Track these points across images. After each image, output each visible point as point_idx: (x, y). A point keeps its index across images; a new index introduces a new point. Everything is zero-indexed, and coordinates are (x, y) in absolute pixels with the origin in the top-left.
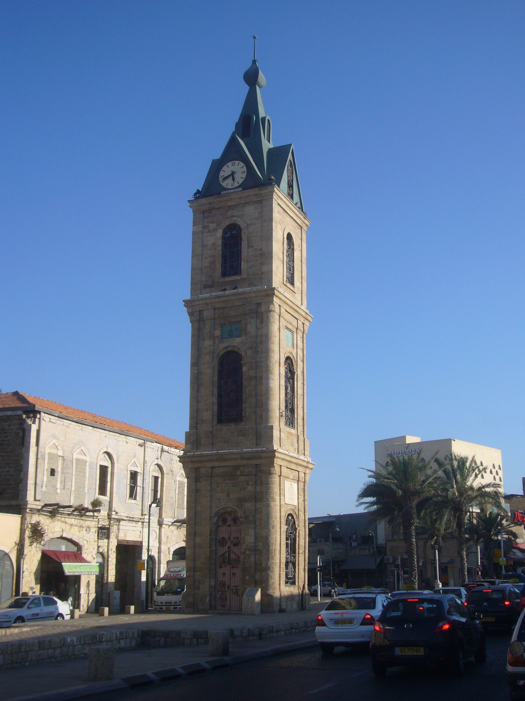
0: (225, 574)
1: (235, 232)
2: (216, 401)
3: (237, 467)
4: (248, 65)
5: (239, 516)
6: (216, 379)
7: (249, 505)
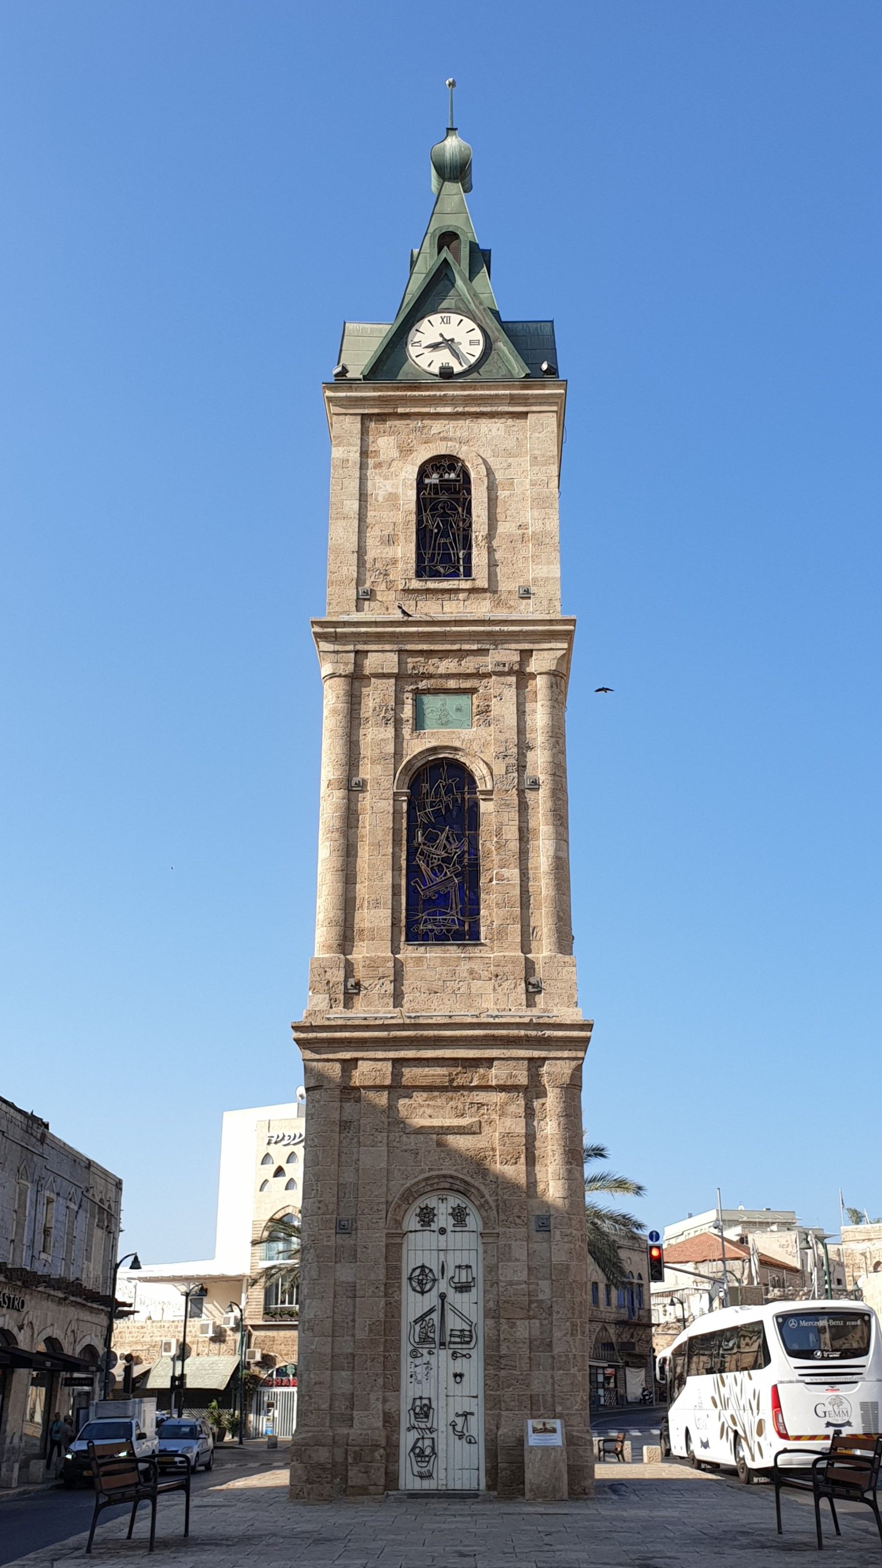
1: (453, 476)
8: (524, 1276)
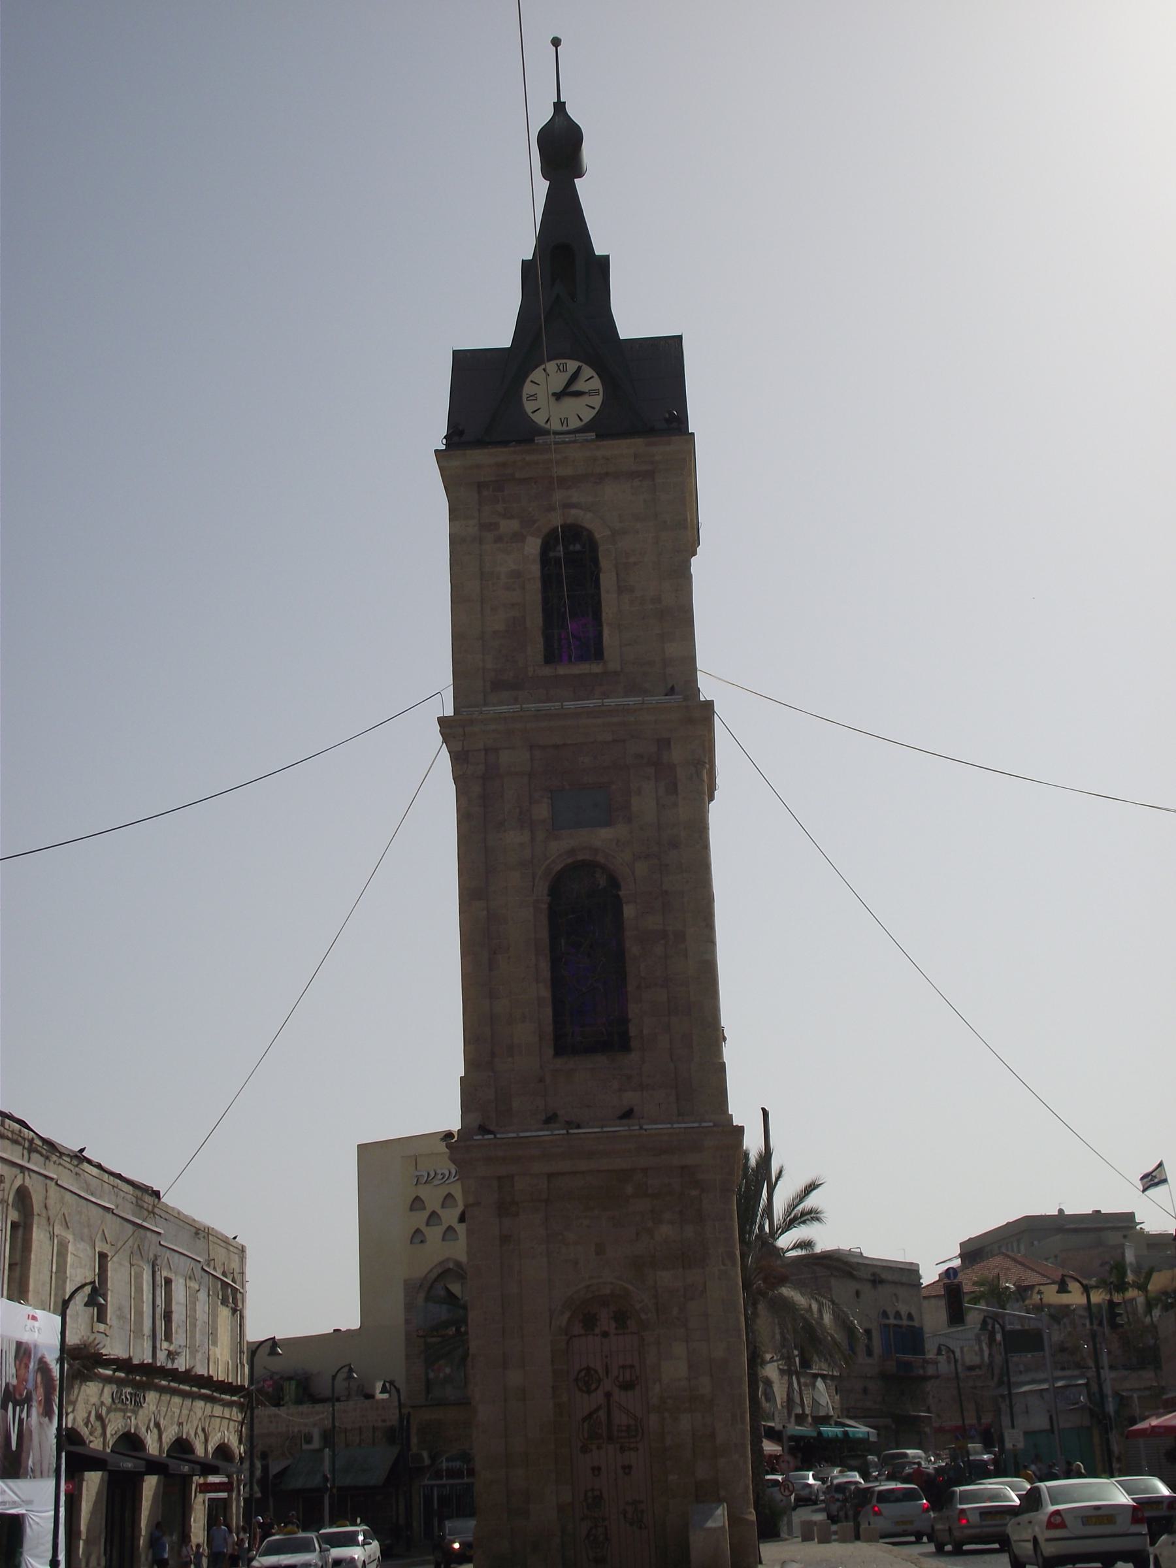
0: (599, 1469)
1: (578, 547)
2: (546, 993)
4: (543, 115)
5: (638, 1306)
6: (544, 934)
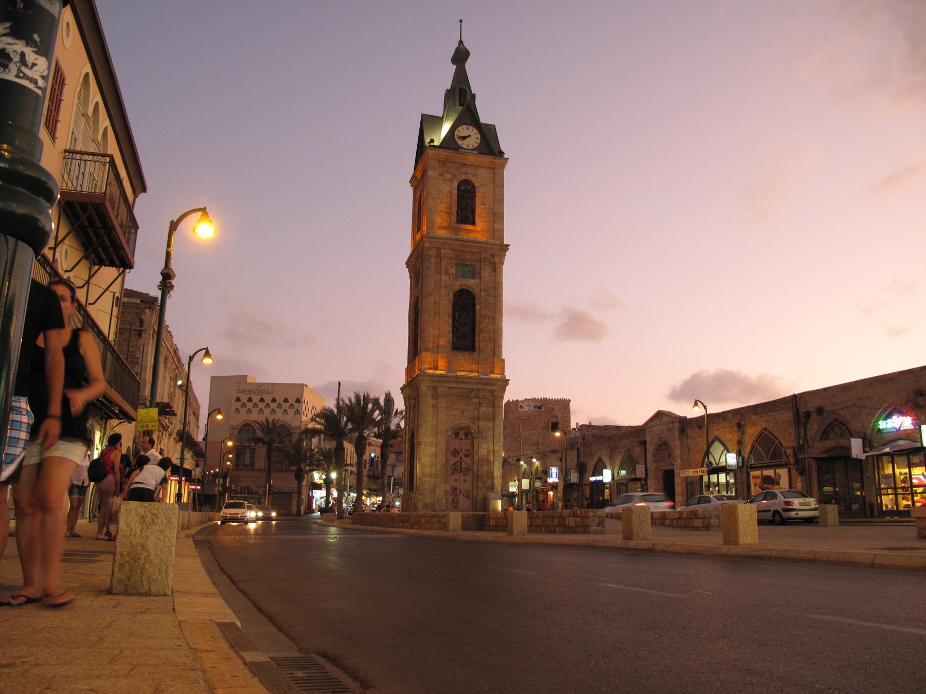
2: (450, 330)
3: (472, 390)
7: (482, 423)
8: (485, 452)
